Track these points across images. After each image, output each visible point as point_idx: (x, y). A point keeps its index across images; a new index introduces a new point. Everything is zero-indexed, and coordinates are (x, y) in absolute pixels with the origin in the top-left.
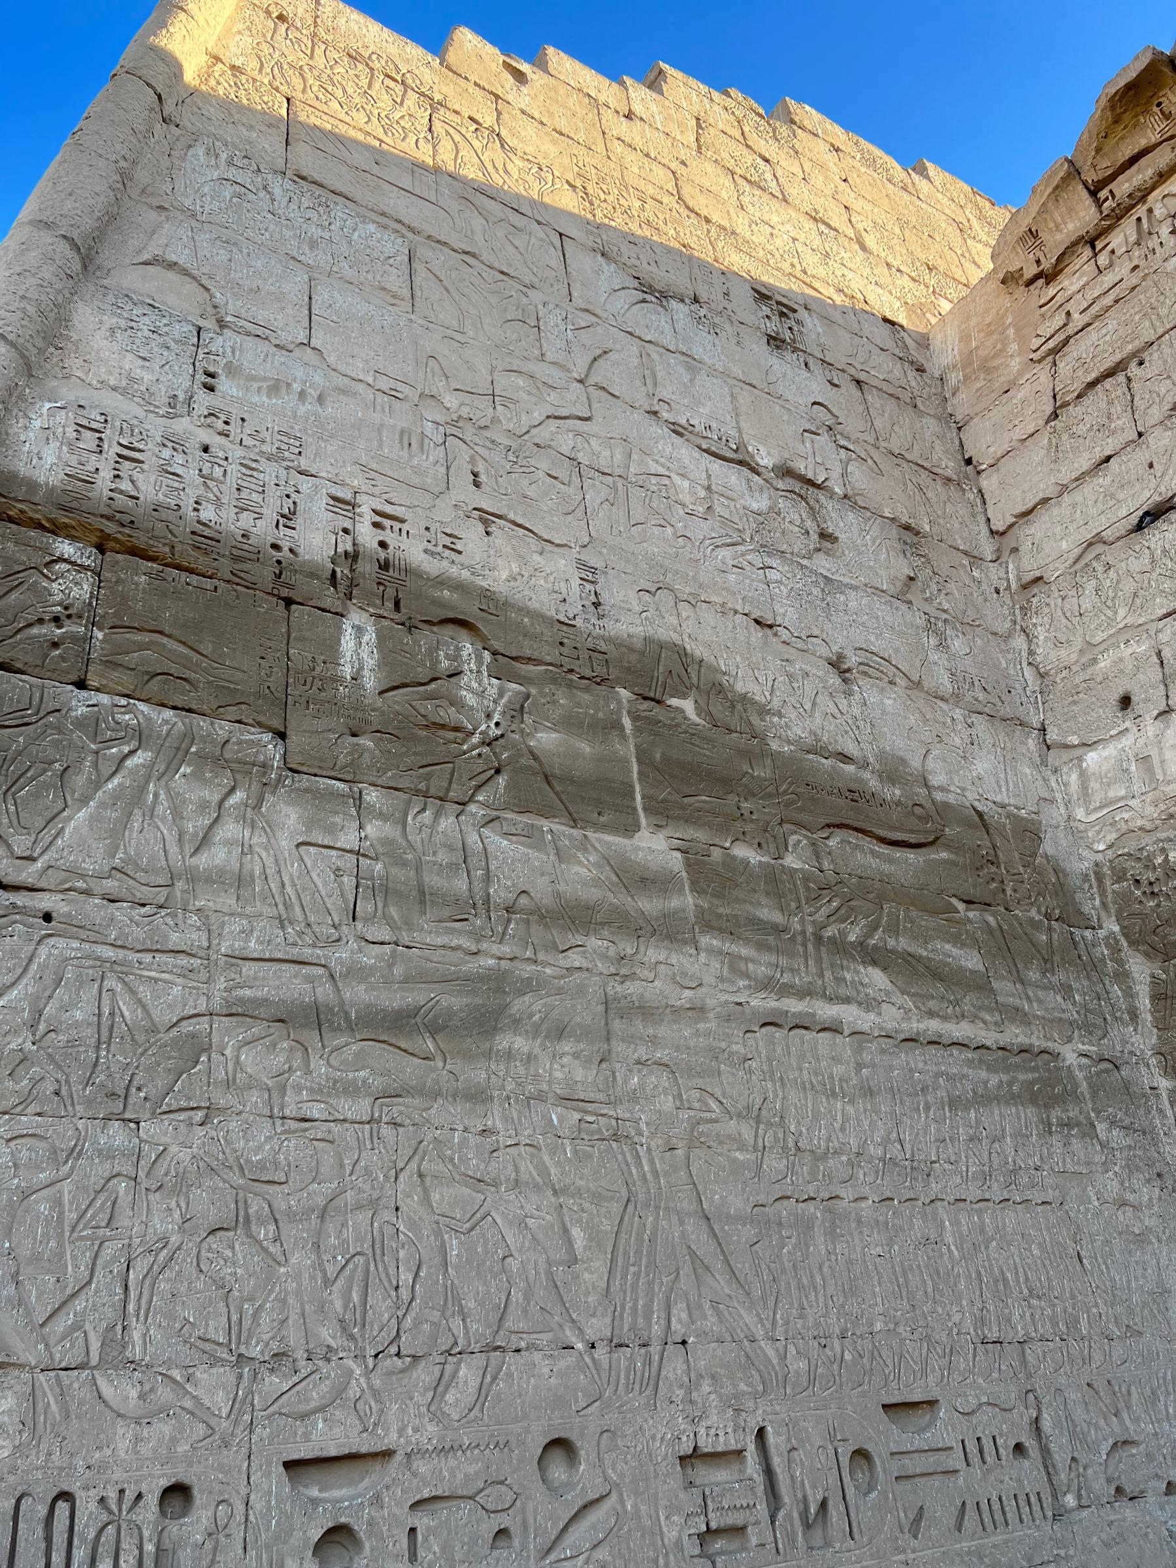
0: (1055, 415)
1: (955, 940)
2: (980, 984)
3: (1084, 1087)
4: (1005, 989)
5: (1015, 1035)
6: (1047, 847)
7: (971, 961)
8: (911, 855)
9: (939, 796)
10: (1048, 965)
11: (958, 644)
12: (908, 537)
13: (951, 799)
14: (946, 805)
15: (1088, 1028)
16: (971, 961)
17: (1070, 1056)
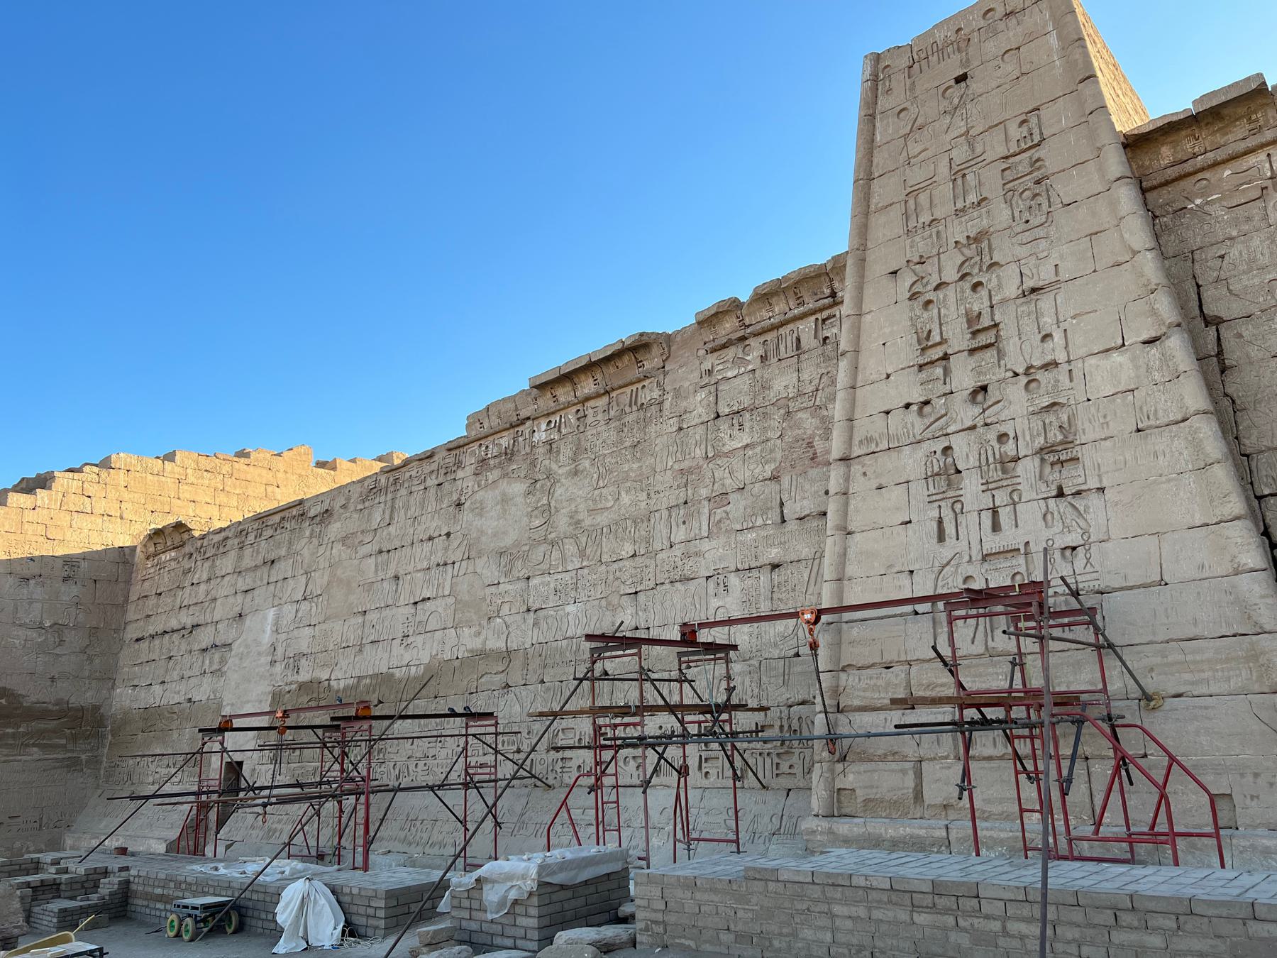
0: (138, 599)
1: (60, 738)
2: (64, 746)
3: (84, 763)
4: (70, 747)
5: (69, 755)
6: (101, 711)
7: (63, 741)
8: (55, 722)
9: (70, 706)
10: (87, 738)
11: (97, 661)
12: (93, 631)
13: (74, 705)
14: (72, 707)
15: (91, 750)
16: (63, 741)
17: (83, 757)
